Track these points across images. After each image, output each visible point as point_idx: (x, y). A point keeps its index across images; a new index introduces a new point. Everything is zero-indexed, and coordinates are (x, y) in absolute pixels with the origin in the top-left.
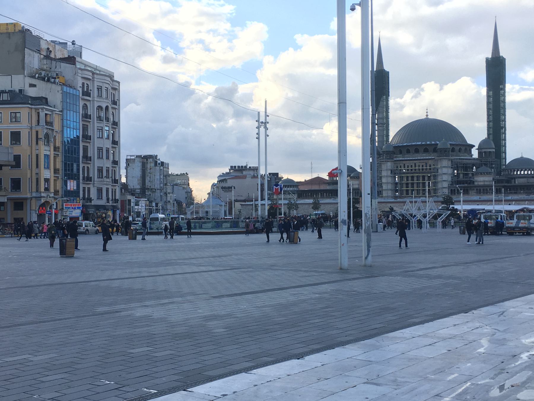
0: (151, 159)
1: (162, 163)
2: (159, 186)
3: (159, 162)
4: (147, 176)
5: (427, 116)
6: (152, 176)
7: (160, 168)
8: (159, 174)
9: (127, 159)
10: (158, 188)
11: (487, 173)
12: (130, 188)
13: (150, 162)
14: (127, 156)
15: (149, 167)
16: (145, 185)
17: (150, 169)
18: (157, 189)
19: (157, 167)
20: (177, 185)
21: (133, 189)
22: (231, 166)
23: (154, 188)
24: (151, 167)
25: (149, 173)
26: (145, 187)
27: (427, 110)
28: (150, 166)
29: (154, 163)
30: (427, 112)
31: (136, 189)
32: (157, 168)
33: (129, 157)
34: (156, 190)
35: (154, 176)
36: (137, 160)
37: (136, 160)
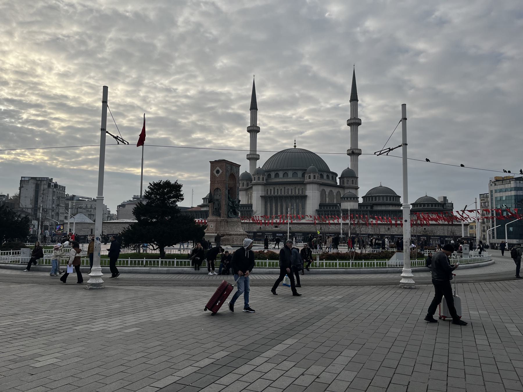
0: (45, 182)
1: (56, 185)
2: (51, 206)
3: (52, 184)
4: (40, 197)
5: (295, 146)
6: (45, 196)
7: (53, 190)
8: (51, 195)
9: (21, 181)
10: (50, 208)
11: (351, 198)
12: (22, 207)
13: (44, 184)
14: (22, 177)
15: (42, 188)
16: (38, 205)
17: (44, 190)
18: (50, 209)
19: (50, 189)
20: (81, 208)
21: (26, 208)
22: (134, 195)
23: (46, 207)
24: (44, 189)
25: (42, 194)
26: (37, 206)
27: (295, 141)
28: (44, 188)
29: (47, 184)
30: (295, 144)
31: (28, 208)
32: (51, 190)
33: (23, 179)
34: (48, 210)
35: (47, 197)
36: (32, 181)
37: (30, 182)
